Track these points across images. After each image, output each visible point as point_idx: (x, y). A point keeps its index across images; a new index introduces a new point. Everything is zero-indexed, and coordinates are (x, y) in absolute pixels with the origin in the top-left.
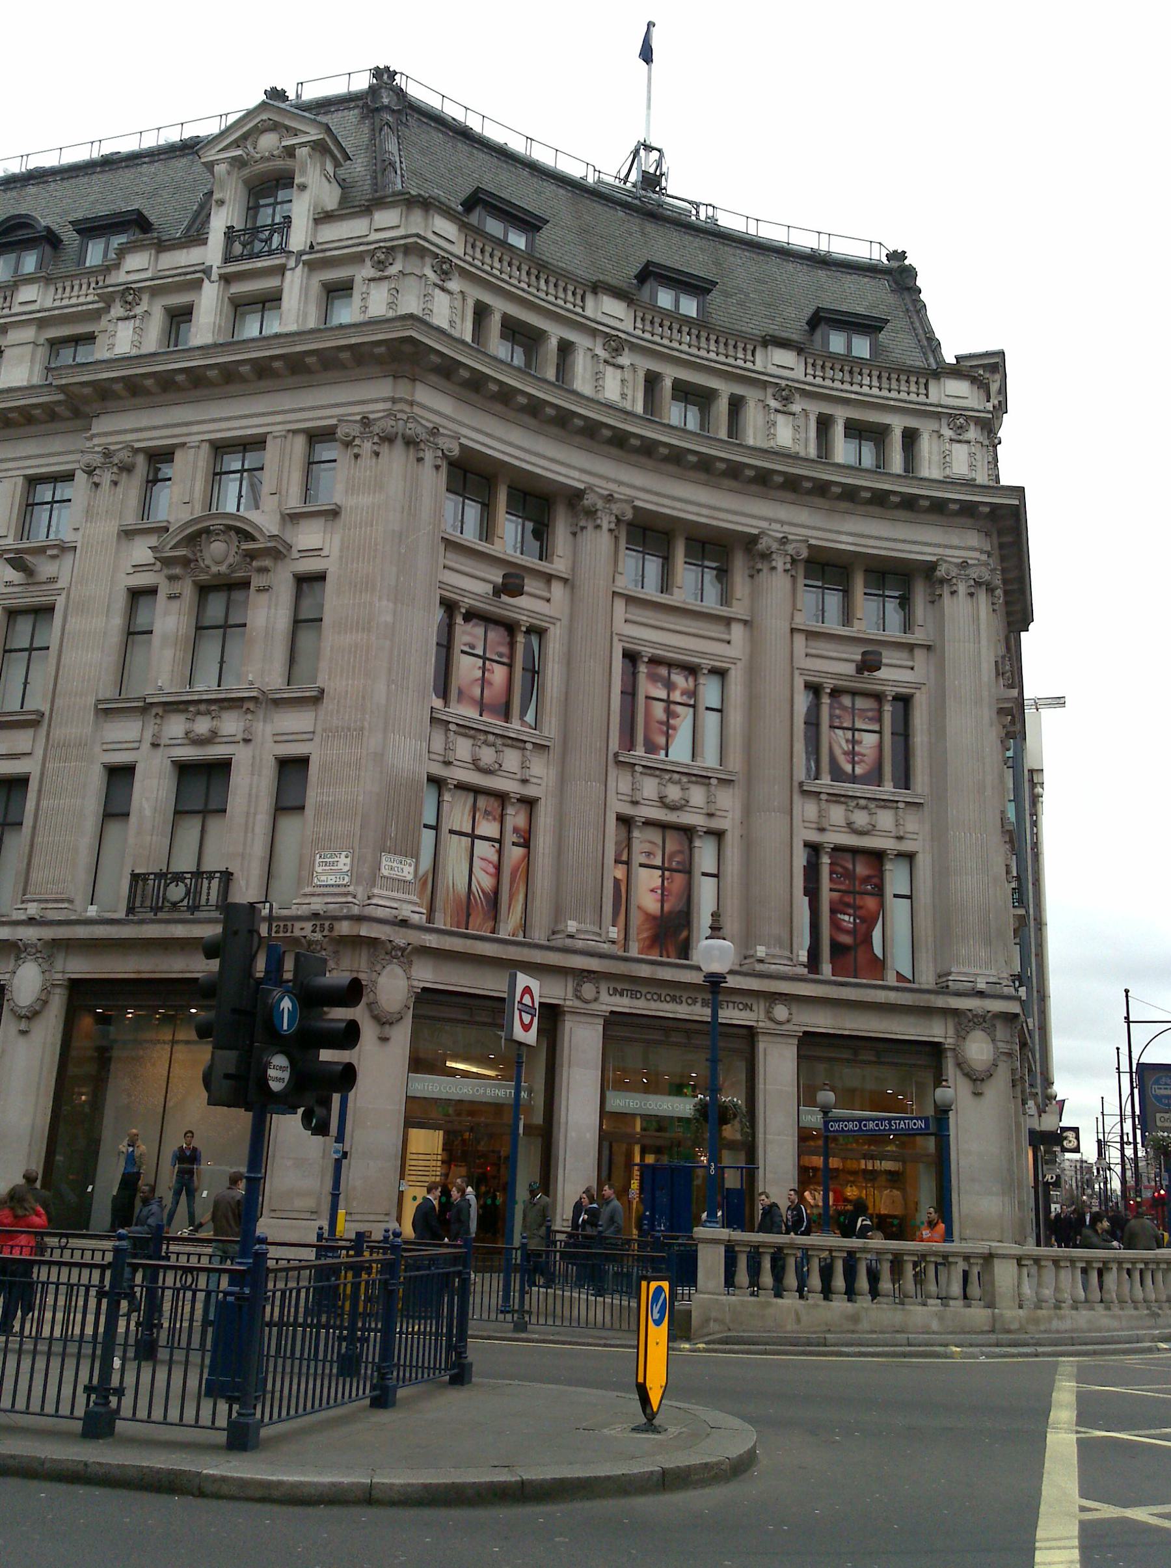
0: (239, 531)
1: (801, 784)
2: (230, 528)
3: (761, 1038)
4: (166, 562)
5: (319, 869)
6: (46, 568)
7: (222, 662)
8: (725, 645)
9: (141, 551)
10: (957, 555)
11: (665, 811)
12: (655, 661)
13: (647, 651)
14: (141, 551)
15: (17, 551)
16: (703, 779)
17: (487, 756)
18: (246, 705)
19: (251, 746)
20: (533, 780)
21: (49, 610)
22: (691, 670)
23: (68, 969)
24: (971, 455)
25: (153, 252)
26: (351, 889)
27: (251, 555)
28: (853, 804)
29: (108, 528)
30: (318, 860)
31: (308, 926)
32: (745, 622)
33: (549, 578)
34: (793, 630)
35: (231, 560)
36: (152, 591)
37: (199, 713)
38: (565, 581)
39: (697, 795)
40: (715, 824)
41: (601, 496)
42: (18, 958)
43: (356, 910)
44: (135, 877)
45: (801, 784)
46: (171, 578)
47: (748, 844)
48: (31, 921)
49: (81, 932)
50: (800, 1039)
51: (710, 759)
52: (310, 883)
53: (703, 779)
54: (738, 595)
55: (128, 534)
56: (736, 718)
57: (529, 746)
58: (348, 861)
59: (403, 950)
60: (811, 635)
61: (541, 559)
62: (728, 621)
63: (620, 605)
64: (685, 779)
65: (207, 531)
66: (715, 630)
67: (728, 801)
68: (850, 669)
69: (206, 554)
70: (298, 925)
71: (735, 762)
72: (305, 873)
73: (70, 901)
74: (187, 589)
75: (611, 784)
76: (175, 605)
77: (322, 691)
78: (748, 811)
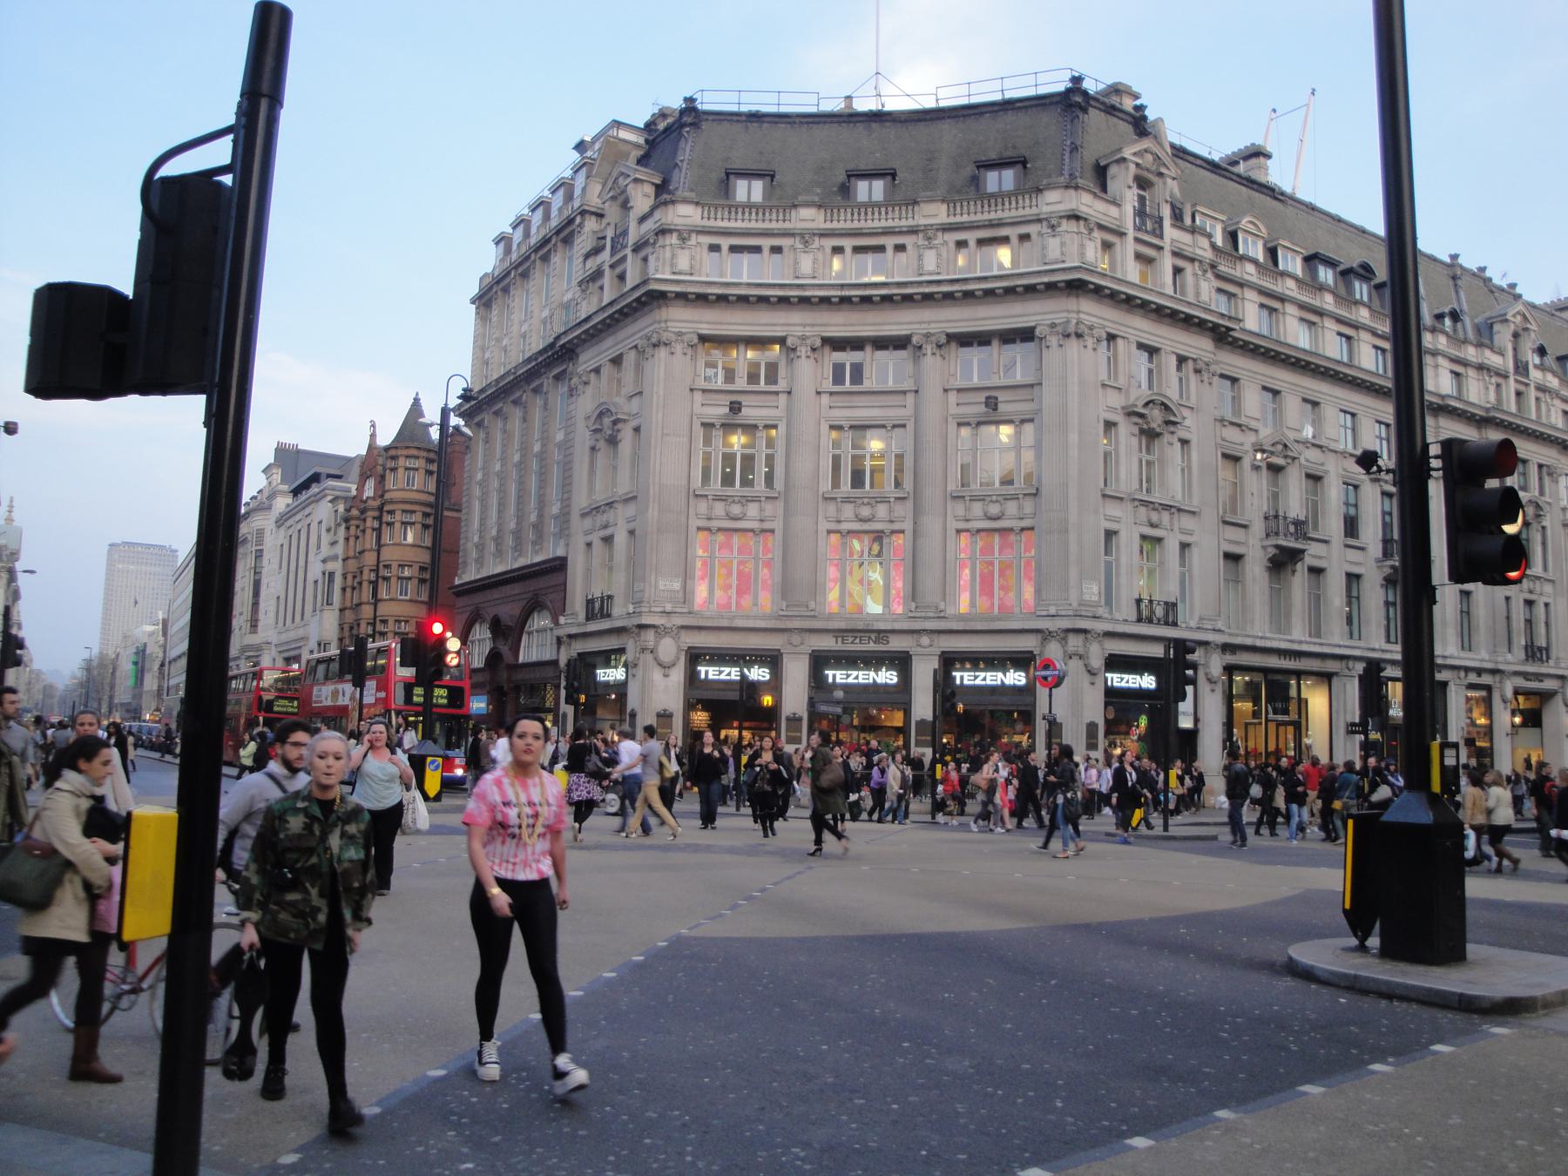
3: (913, 657)
10: (1049, 319)
17: (736, 510)
24: (1063, 244)
34: (946, 390)
40: (896, 526)
41: (799, 337)
50: (940, 656)
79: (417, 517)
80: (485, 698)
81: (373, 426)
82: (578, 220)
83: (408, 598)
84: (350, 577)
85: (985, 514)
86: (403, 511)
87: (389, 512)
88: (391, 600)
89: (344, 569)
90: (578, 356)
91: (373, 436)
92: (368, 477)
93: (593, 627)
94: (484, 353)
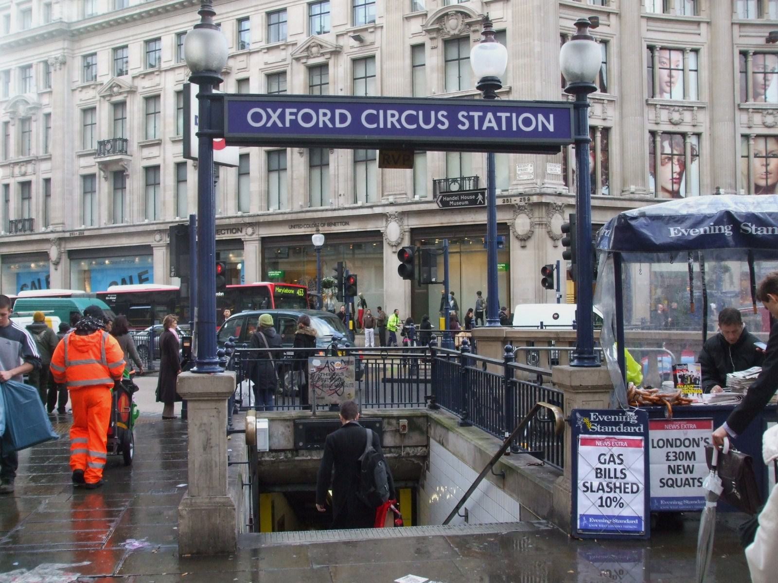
0: (462, 13)
1: (739, 105)
4: (428, 31)
5: (519, 172)
6: (368, 37)
7: (459, 77)
8: (697, 36)
9: (416, 26)
11: (672, 126)
12: (662, 48)
13: (659, 45)
14: (416, 26)
15: (355, 31)
16: (690, 108)
20: (609, 118)
21: (373, 57)
22: (682, 50)
23: (410, 224)
26: (534, 181)
28: (765, 112)
29: (398, 17)
30: (518, 168)
31: (518, 199)
32: (708, 23)
33: (608, 14)
34: (732, 24)
35: (459, 27)
36: (422, 46)
38: (617, 14)
39: (687, 116)
40: (696, 130)
42: (387, 220)
43: (538, 191)
44: (434, 181)
45: (739, 105)
46: (432, 39)
47: (713, 139)
48: (391, 204)
49: (415, 208)
51: (692, 97)
52: (515, 179)
53: (690, 108)
54: (703, 8)
55: (408, 18)
56: (705, 74)
57: (606, 102)
58: (532, 168)
59: (560, 207)
60: (742, 25)
61: (603, 5)
62: (698, 23)
63: (644, 22)
64: (681, 109)
65: (447, 14)
66: (692, 28)
67: (703, 117)
68: (762, 41)
69: (447, 26)
70: (513, 199)
71: (705, 98)
72: (512, 175)
73: (406, 194)
74: (440, 44)
75: (646, 115)
76: (435, 51)
77: (510, 88)
78: (712, 121)
85: (764, 123)
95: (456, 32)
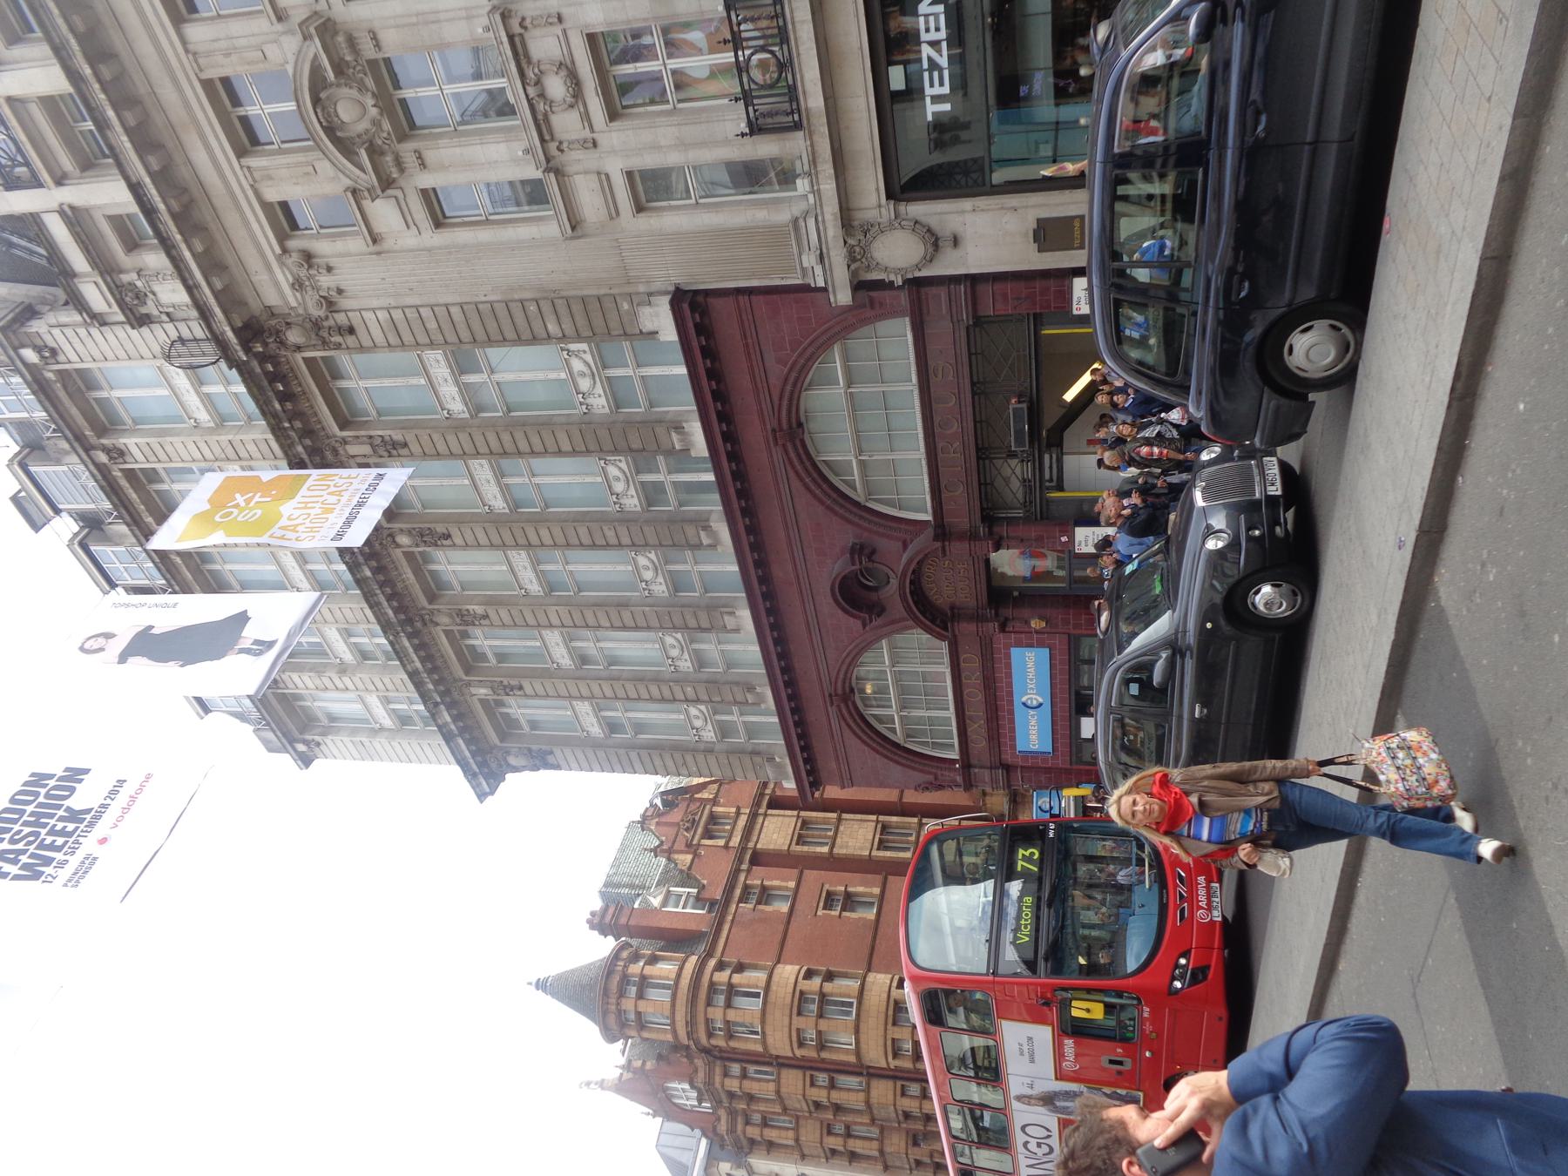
2: (316, 101)
18: (517, 30)
19: (565, 11)
25: (76, 280)
27: (340, 68)
37: (542, 95)
65: (330, 131)
79: (722, 977)
80: (1015, 652)
81: (588, 1084)
82: (30, 355)
83: (855, 1001)
84: (833, 1142)
86: (709, 1003)
87: (710, 1035)
88: (857, 1031)
89: (819, 1157)
90: (270, 311)
91: (602, 1085)
92: (669, 1098)
93: (814, 100)
94: (382, 729)
95: (370, 101)
